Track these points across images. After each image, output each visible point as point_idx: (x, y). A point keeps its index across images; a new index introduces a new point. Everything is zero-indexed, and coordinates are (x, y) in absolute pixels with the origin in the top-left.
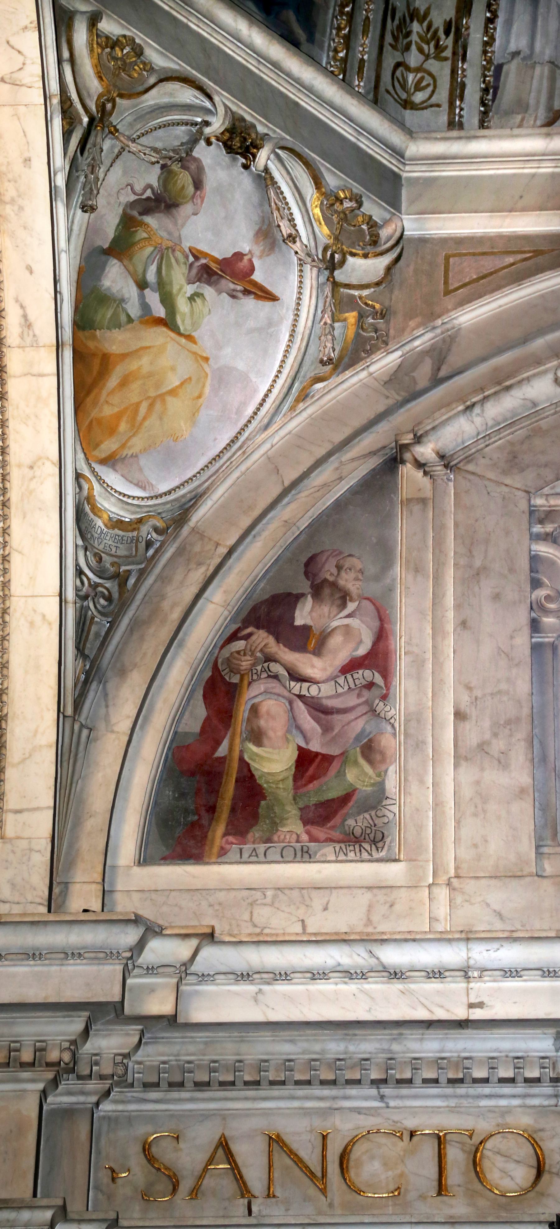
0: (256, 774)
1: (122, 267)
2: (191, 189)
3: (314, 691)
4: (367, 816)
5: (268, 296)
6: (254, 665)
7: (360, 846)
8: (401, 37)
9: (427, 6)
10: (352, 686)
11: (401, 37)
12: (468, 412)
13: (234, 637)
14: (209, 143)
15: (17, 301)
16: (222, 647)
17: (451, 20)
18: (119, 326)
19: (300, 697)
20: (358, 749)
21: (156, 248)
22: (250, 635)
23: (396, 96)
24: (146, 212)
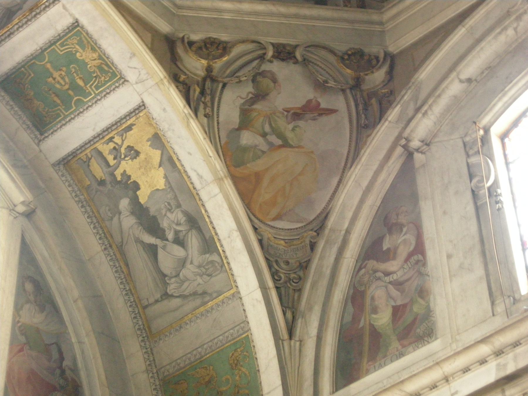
0: (377, 327)
1: (250, 132)
2: (272, 85)
3: (395, 277)
4: (424, 324)
5: (331, 111)
6: (369, 278)
7: (423, 340)
10: (410, 266)
12: (426, 116)
13: (360, 269)
14: (271, 62)
15: (192, 169)
16: (356, 276)
18: (259, 157)
19: (390, 283)
20: (417, 294)
21: (265, 116)
22: (366, 265)
24: (253, 103)
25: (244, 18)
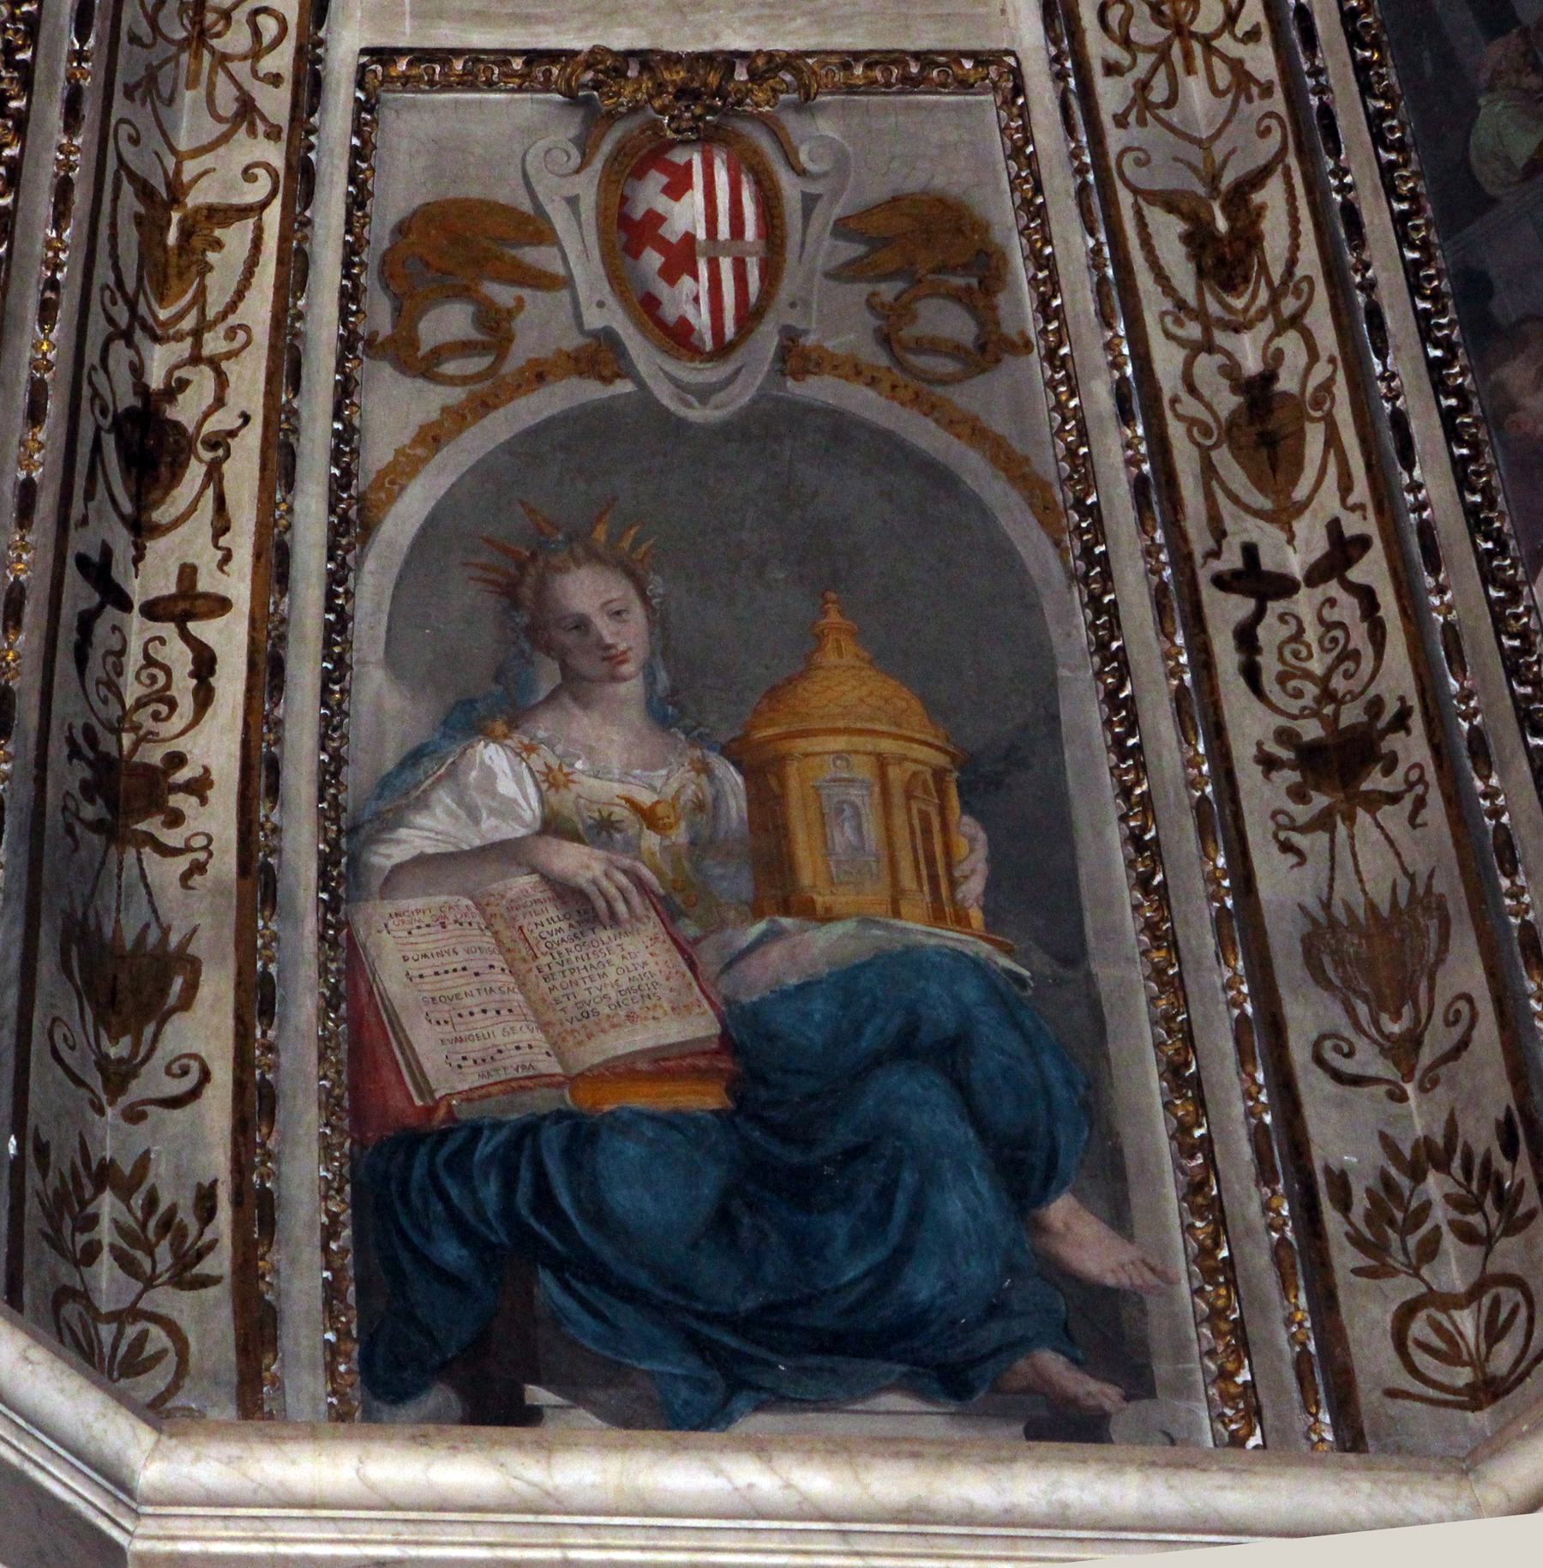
8: (1393, 1236)
9: (1445, 1116)
11: (1393, 1236)
17: (1508, 1109)
23: (1431, 1392)
25: (573, 1554)
